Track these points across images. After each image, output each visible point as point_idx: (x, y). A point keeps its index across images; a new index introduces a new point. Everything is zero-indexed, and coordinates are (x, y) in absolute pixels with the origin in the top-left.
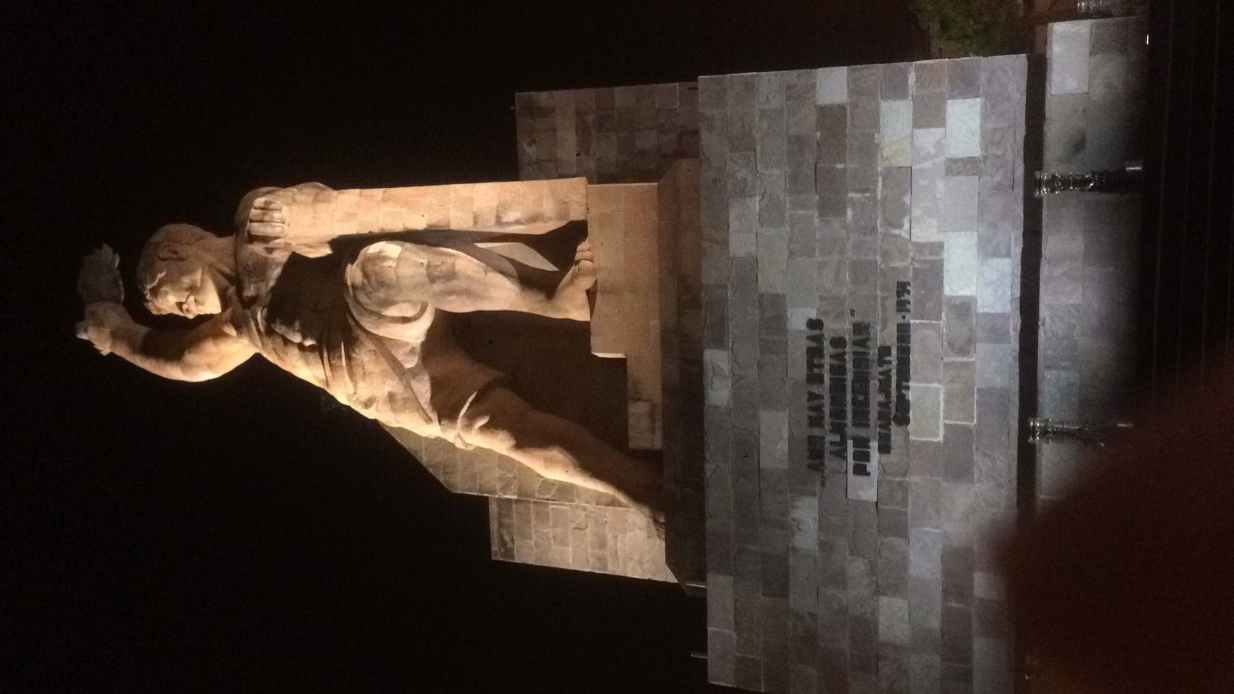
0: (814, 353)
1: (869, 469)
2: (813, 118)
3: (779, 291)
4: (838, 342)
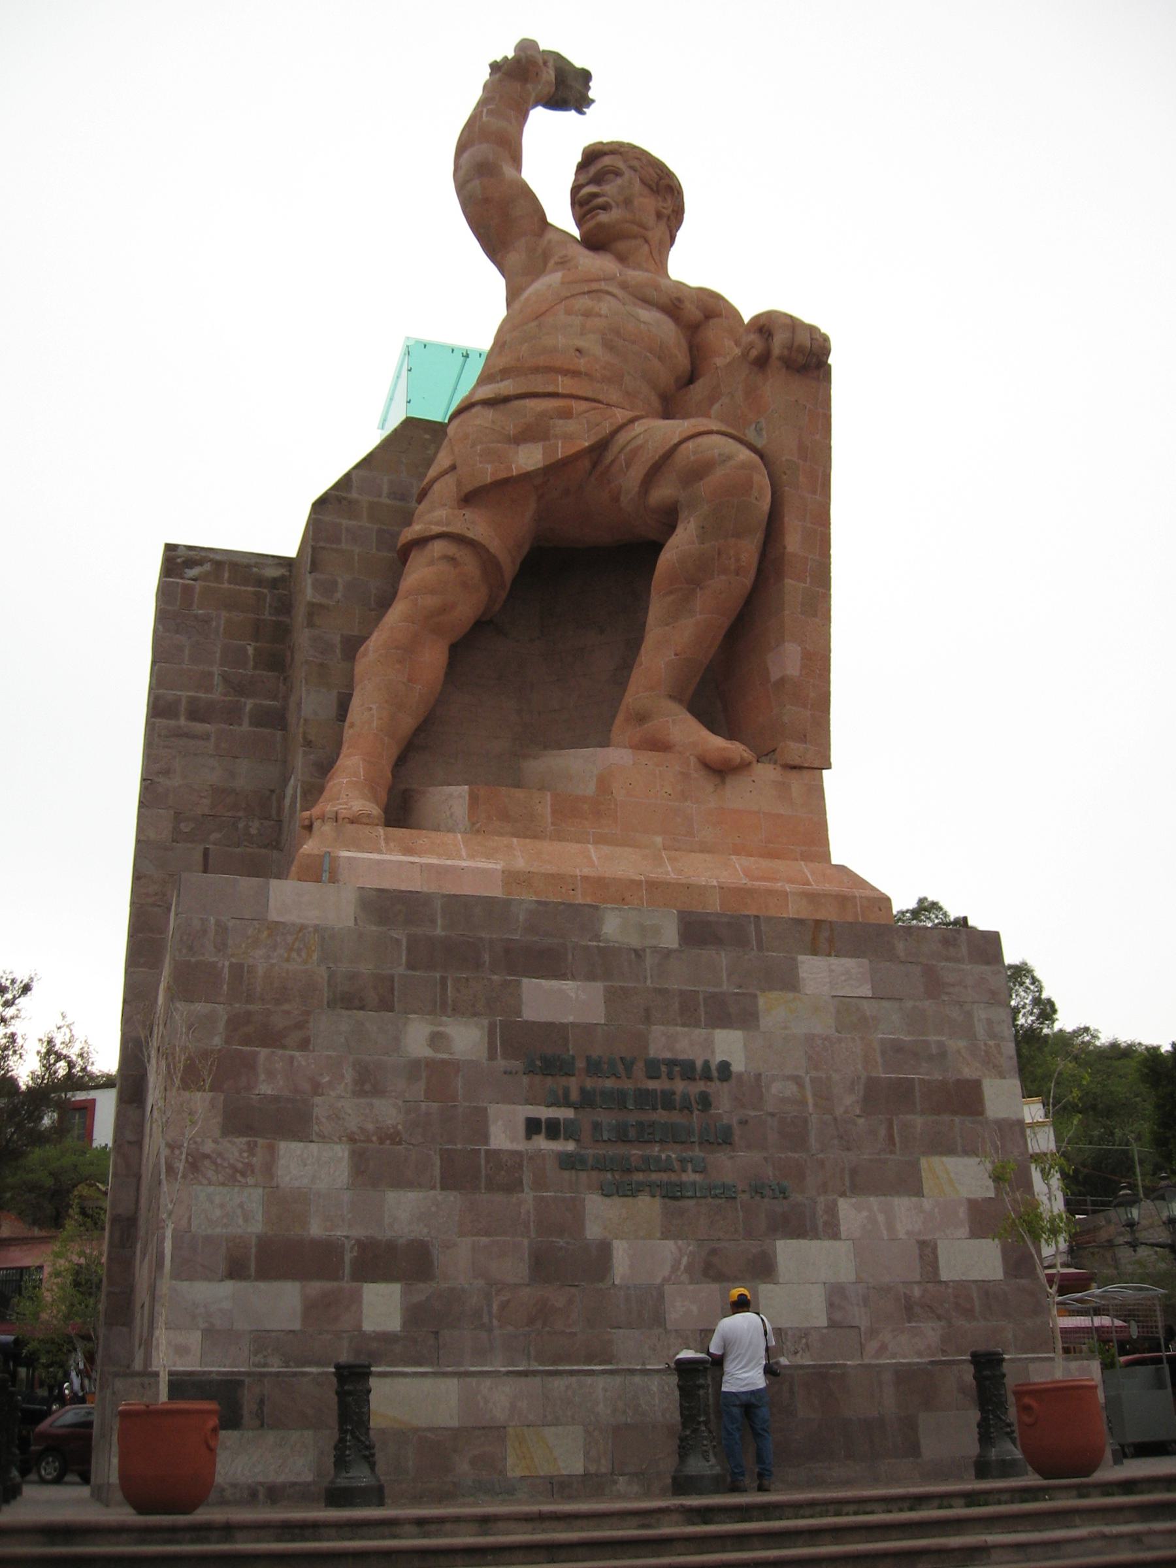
0: (687, 1070)
1: (535, 1137)
2: (968, 1073)
3: (762, 1022)
4: (705, 1101)
